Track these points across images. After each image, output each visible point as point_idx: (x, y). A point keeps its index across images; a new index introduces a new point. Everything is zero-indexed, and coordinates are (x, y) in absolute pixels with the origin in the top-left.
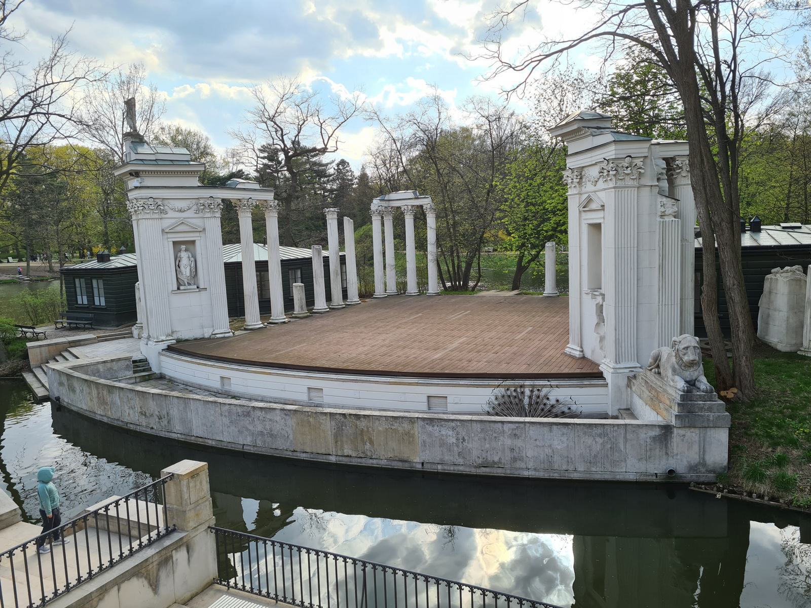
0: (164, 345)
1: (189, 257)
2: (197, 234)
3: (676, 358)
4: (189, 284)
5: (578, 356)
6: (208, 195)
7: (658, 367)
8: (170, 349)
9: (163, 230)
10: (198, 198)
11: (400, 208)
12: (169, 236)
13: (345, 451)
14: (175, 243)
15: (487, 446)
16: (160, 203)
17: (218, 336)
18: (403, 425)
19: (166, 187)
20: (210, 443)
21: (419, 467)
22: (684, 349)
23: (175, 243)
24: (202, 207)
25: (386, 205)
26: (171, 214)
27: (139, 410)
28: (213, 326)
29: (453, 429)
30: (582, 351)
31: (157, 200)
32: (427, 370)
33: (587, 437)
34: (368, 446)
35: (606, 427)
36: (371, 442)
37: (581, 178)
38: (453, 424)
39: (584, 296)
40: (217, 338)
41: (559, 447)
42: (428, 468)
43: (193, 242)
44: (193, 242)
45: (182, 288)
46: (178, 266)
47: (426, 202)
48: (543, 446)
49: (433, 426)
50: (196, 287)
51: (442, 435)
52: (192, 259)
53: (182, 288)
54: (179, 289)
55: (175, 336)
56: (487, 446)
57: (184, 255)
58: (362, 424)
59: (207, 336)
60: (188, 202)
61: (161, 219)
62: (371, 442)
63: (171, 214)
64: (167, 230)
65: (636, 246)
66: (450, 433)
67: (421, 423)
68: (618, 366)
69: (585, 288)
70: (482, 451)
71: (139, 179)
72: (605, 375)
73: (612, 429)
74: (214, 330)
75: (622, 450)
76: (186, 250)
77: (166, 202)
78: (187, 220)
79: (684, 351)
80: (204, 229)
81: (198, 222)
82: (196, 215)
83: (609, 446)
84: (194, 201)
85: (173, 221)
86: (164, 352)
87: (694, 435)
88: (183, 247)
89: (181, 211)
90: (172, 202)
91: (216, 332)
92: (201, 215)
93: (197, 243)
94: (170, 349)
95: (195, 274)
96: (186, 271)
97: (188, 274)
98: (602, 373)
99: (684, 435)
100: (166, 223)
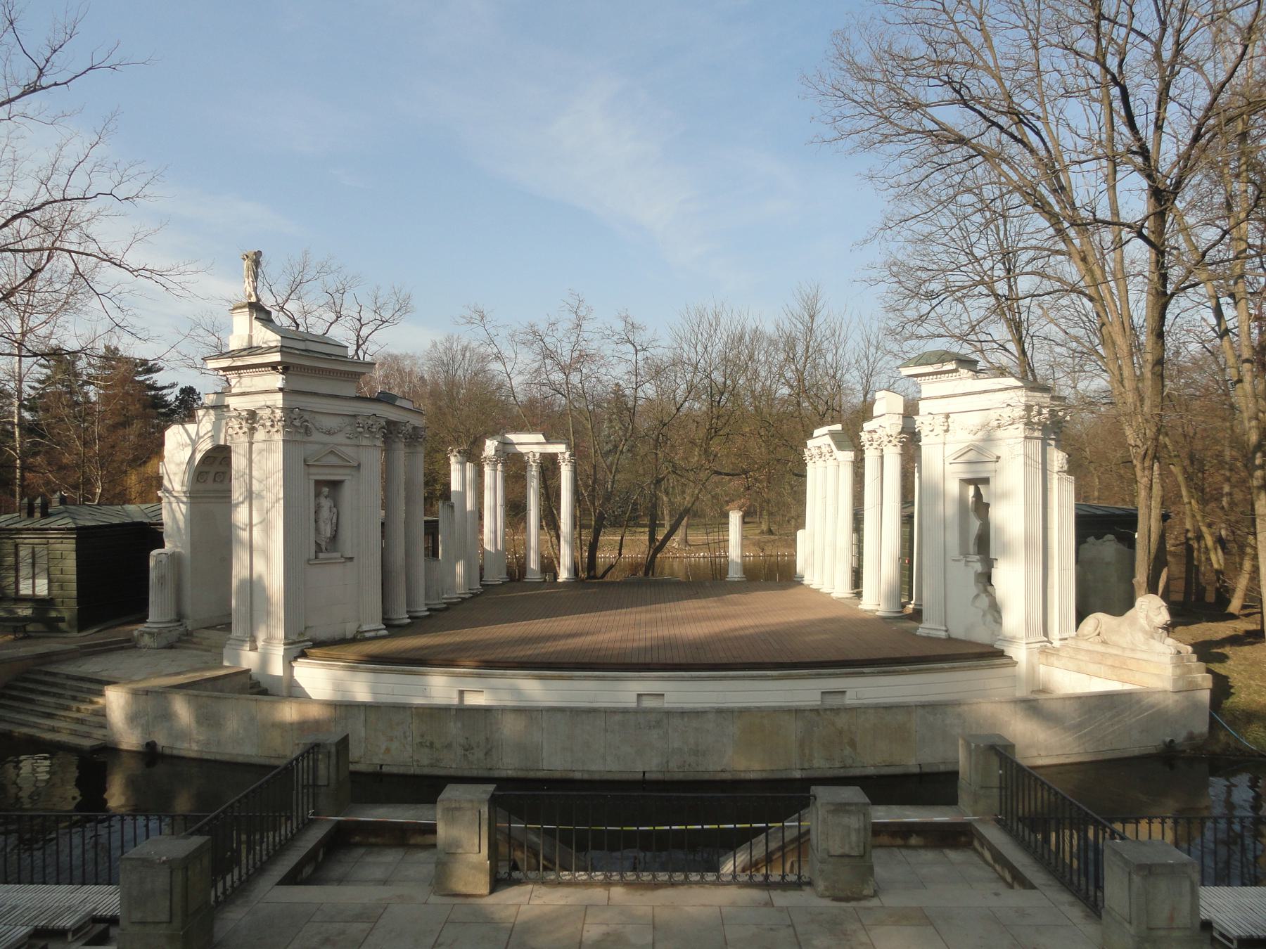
2: (348, 471)
12: (312, 470)
14: (319, 483)
19: (316, 394)
20: (578, 776)
26: (316, 436)
27: (419, 740)
32: (825, 658)
34: (848, 751)
36: (853, 744)
45: (321, 555)
47: (559, 448)
58: (842, 721)
60: (338, 420)
69: (954, 550)
80: (359, 465)
81: (349, 452)
82: (348, 442)
84: (347, 420)
88: (326, 490)
89: (329, 433)
90: (319, 417)
91: (365, 628)
92: (354, 442)
95: (334, 538)
96: (327, 531)
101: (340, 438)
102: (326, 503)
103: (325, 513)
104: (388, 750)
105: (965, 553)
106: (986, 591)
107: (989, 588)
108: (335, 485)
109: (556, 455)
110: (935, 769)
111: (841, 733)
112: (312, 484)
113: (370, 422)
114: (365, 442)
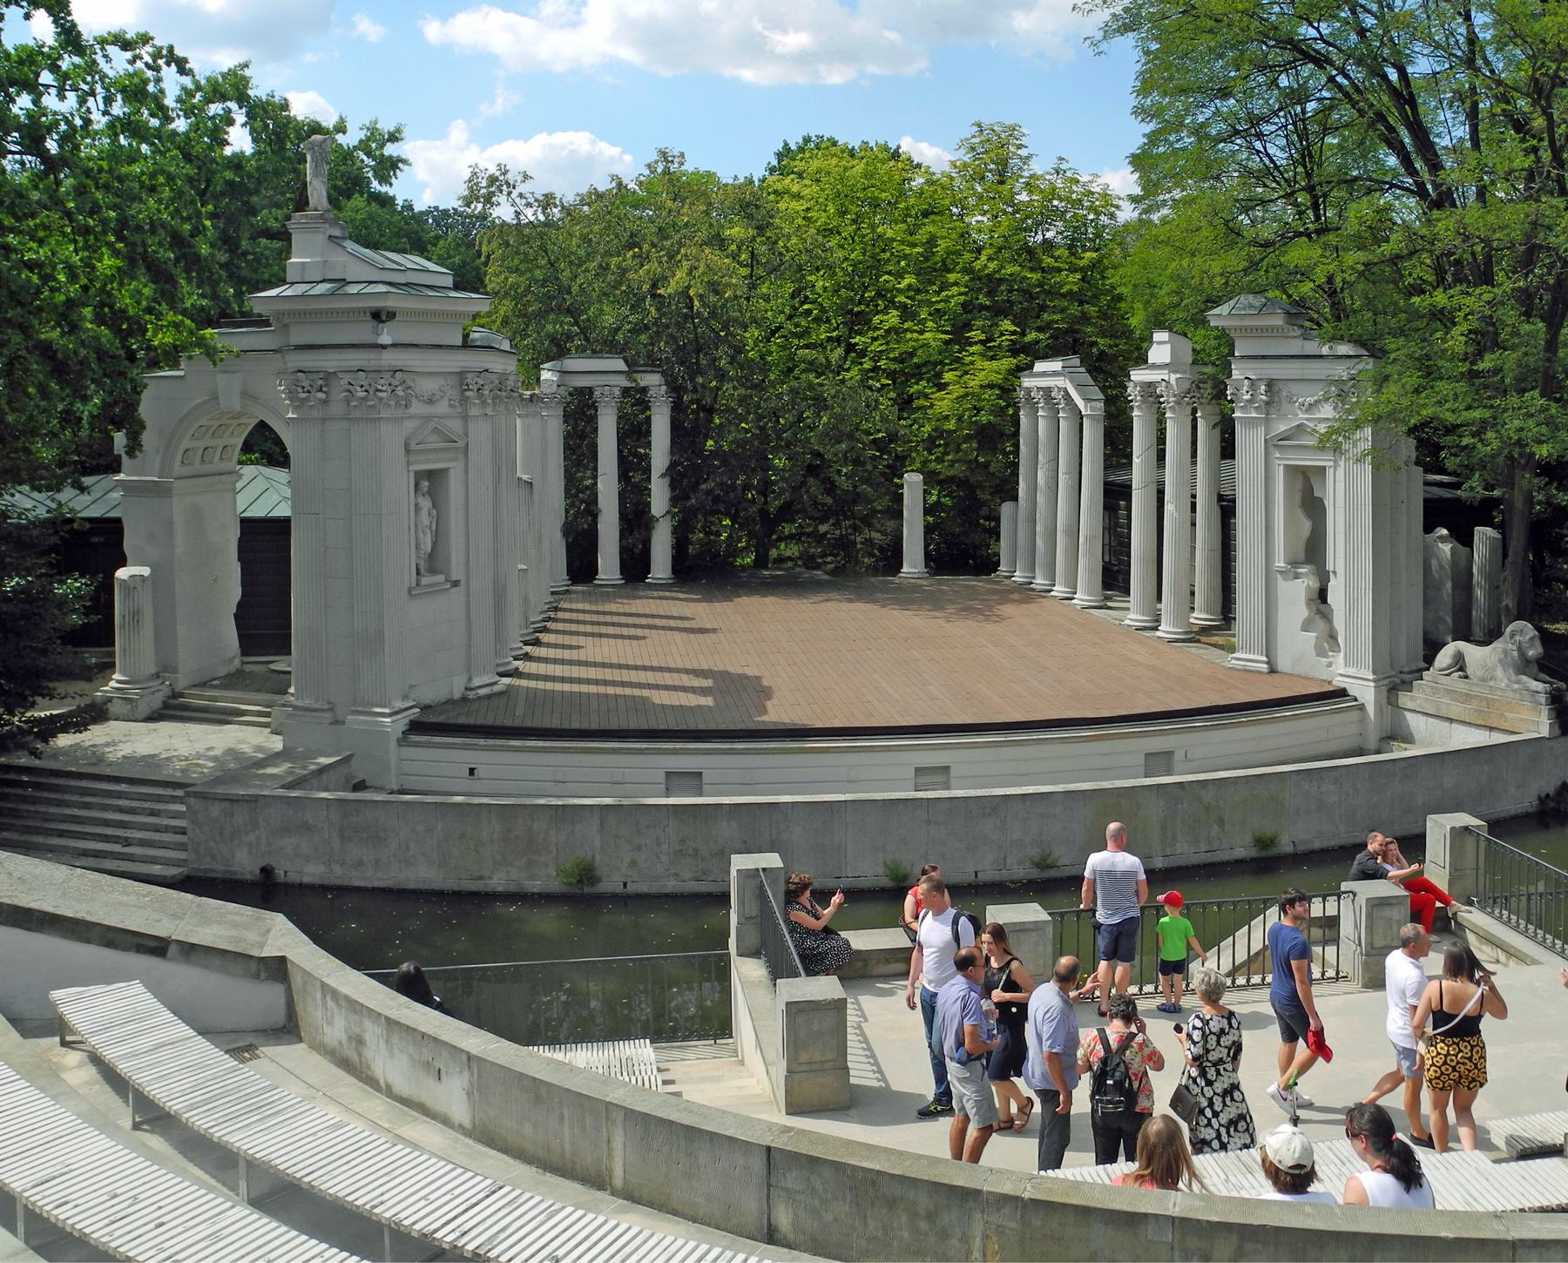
0: (402, 723)
11: (591, 390)
17: (482, 692)
26: (417, 408)
28: (469, 671)
31: (406, 376)
34: (1215, 830)
40: (480, 698)
42: (1301, 848)
44: (444, 471)
45: (425, 581)
47: (652, 380)
58: (1208, 796)
59: (457, 696)
66: (1332, 788)
74: (470, 679)
81: (455, 425)
89: (431, 401)
91: (477, 682)
93: (452, 473)
96: (427, 546)
101: (442, 408)
102: (426, 503)
104: (633, 864)
105: (1294, 563)
106: (1319, 612)
107: (1322, 607)
109: (644, 390)
110: (1310, 847)
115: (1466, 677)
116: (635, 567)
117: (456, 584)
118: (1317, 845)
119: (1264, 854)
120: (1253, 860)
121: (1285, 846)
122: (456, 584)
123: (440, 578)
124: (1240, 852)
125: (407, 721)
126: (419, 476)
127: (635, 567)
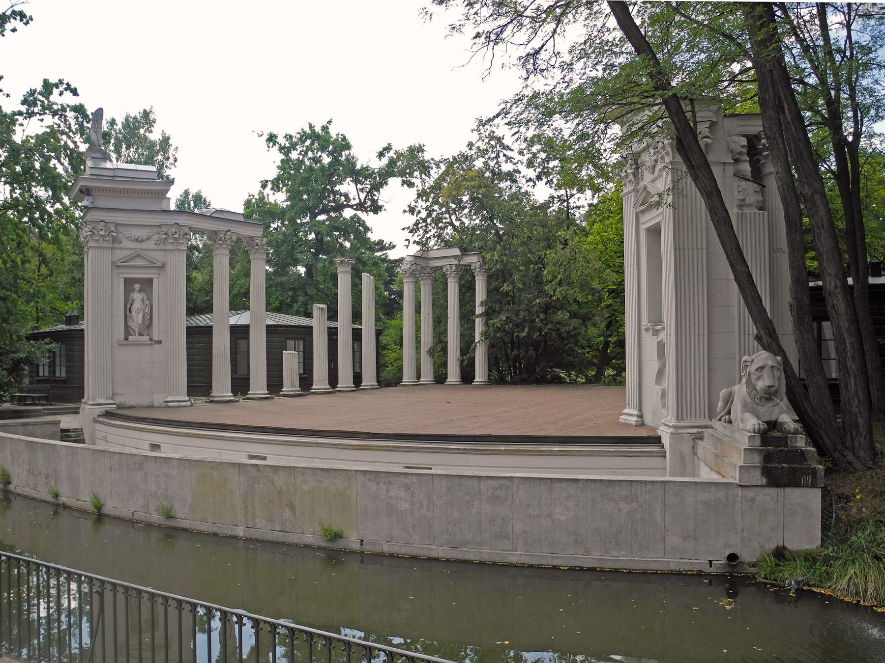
0: (100, 410)
1: (143, 300)
2: (156, 271)
3: (747, 387)
4: (140, 334)
5: (634, 423)
6: (172, 222)
7: (729, 413)
8: (108, 414)
9: (113, 263)
10: (160, 226)
11: (441, 268)
12: (121, 270)
13: (257, 520)
15: (456, 515)
16: (113, 228)
17: (170, 404)
18: (337, 482)
19: (125, 210)
21: (356, 546)
22: (757, 370)
23: (126, 280)
24: (164, 236)
25: (423, 265)
26: (126, 244)
29: (407, 487)
30: (641, 416)
33: (606, 501)
34: (288, 513)
35: (634, 485)
36: (292, 507)
37: (637, 168)
38: (406, 480)
39: (644, 334)
41: (563, 518)
42: (368, 548)
43: (151, 281)
44: (151, 281)
46: (128, 310)
48: (539, 516)
49: (378, 483)
50: (148, 338)
51: (391, 498)
52: (147, 302)
53: (130, 338)
54: (126, 339)
55: (118, 400)
56: (456, 515)
57: (137, 296)
58: (280, 480)
61: (112, 248)
62: (292, 507)
63: (126, 244)
64: (119, 264)
65: (704, 246)
67: (361, 478)
68: (682, 424)
70: (448, 522)
71: (91, 198)
72: (663, 441)
73: (644, 489)
75: (659, 521)
76: (140, 291)
77: (121, 229)
78: (148, 253)
79: (758, 373)
82: (157, 247)
83: (639, 516)
84: (155, 230)
85: (127, 253)
86: (101, 419)
87: (768, 499)
88: (137, 286)
89: (138, 240)
90: (129, 229)
91: (169, 399)
92: (162, 247)
93: (155, 282)
94: (108, 414)
95: (148, 324)
96: (137, 318)
97: (140, 321)
98: (660, 437)
99: (753, 500)
100: (120, 254)
101: (150, 244)
103: (137, 305)
108: (147, 284)
110: (378, 549)
111: (280, 493)
112: (122, 281)
113: (174, 230)
114: (169, 247)
115: (730, 422)
116: (467, 376)
117: (160, 342)
118: (386, 549)
119: (331, 545)
120: (319, 548)
121: (352, 542)
122: (160, 342)
123: (145, 338)
124: (309, 538)
125: (103, 410)
126: (129, 283)
127: (467, 376)
